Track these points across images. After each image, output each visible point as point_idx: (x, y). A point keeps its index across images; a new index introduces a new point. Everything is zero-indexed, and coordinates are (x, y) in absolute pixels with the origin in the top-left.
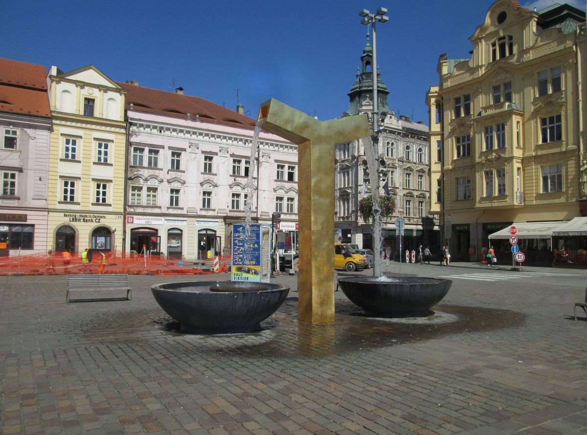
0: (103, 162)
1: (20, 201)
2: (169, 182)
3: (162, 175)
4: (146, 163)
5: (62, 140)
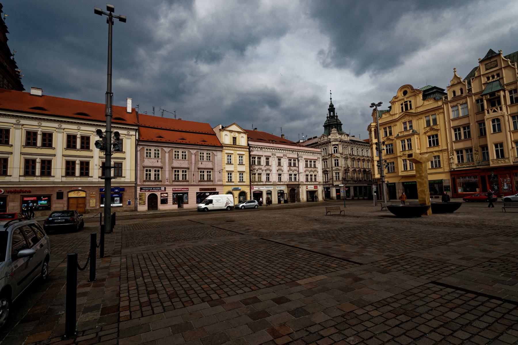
0: (241, 164)
1: (213, 182)
2: (266, 170)
3: (263, 168)
4: (256, 163)
5: (226, 156)
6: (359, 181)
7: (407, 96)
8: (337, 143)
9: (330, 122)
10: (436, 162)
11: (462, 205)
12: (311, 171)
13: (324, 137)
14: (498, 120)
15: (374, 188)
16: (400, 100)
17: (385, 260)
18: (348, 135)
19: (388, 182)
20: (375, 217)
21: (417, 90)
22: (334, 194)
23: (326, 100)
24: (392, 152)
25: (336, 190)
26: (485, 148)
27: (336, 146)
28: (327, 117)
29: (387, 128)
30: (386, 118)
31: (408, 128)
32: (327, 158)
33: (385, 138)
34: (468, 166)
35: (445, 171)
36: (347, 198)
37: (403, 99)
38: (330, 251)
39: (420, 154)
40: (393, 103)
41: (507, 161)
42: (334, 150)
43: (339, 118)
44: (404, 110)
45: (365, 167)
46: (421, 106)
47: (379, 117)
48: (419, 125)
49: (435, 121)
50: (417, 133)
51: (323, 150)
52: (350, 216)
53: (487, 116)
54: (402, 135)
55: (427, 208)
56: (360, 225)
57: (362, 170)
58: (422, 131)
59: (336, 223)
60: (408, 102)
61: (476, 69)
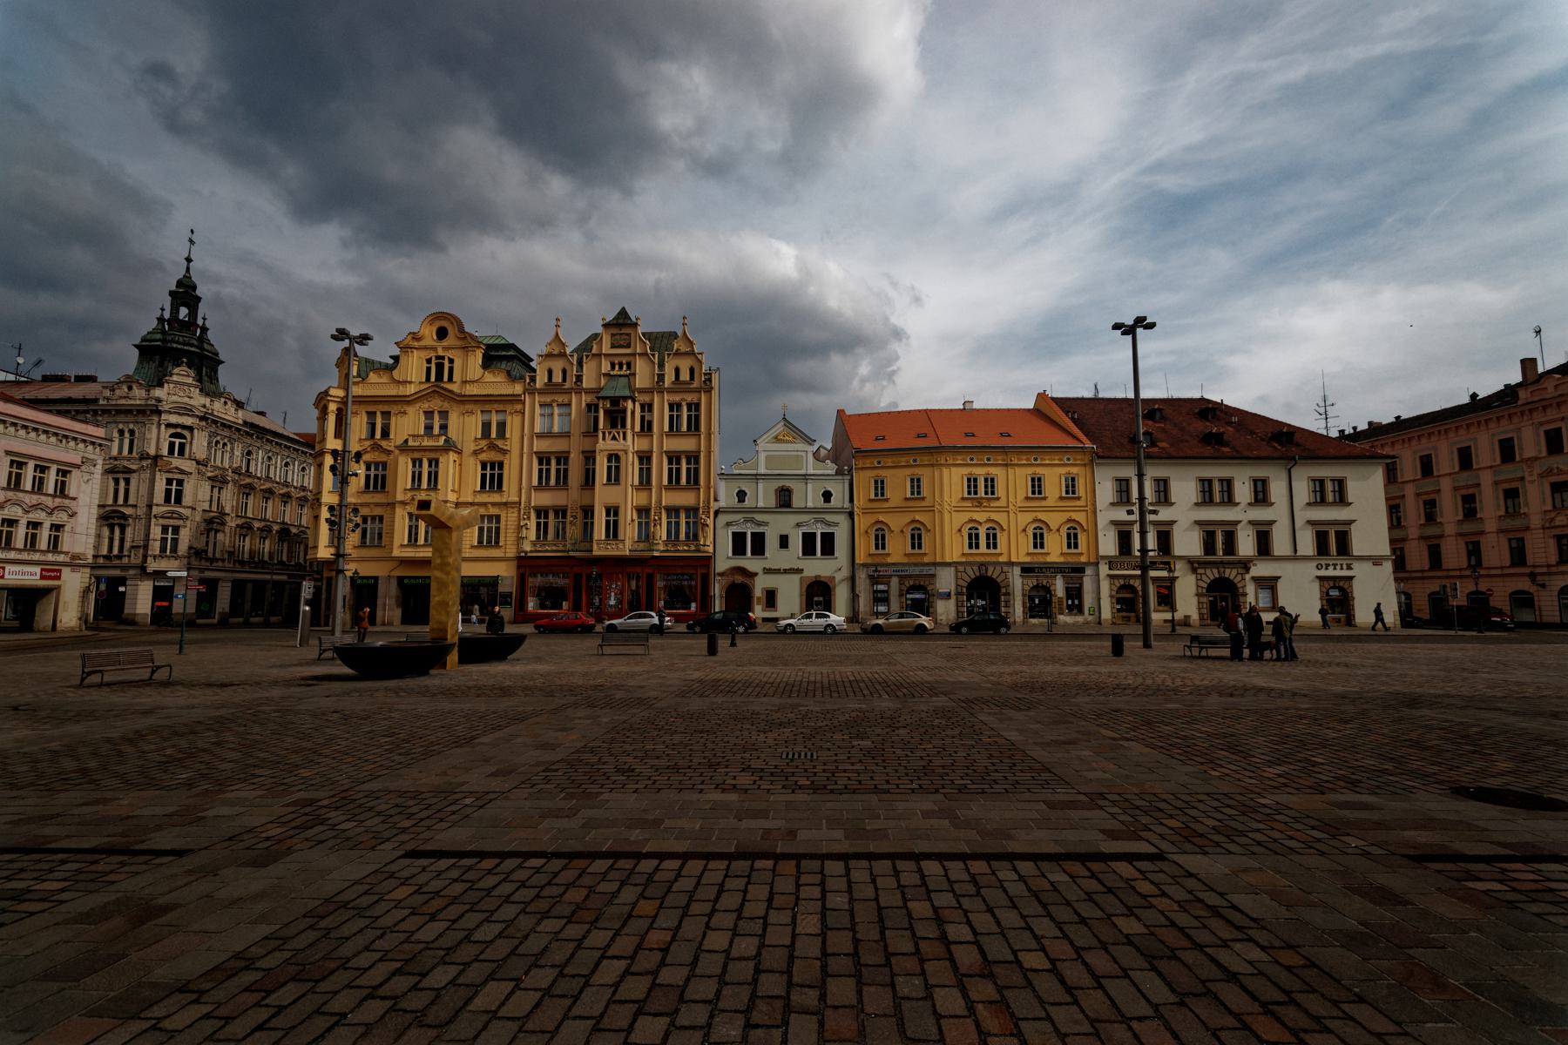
6: (256, 562)
7: (445, 343)
8: (188, 421)
9: (172, 341)
10: (490, 530)
11: (527, 642)
12: (36, 507)
13: (130, 388)
14: (618, 458)
15: (307, 589)
16: (425, 348)
17: (281, 820)
18: (239, 405)
19: (356, 572)
20: (288, 683)
21: (471, 336)
22: (142, 600)
23: (170, 252)
24: (383, 486)
25: (156, 589)
26: (588, 511)
27: (179, 431)
28: (161, 320)
29: (379, 414)
30: (377, 386)
31: (436, 430)
32: (134, 467)
33: (368, 443)
34: (554, 548)
35: (508, 555)
36: (199, 621)
37: (434, 349)
38: (49, 831)
39: (457, 505)
40: (405, 348)
41: (621, 546)
42: (172, 445)
43: (210, 335)
44: (433, 378)
45: (287, 520)
46: (477, 381)
47: (359, 375)
48: (466, 427)
49: (502, 426)
50: (456, 447)
51: (116, 434)
52: (192, 685)
53: (601, 445)
54: (417, 444)
55: (447, 649)
56: (223, 712)
57: (276, 528)
58: (469, 447)
59: (115, 716)
60: (446, 359)
61: (595, 336)
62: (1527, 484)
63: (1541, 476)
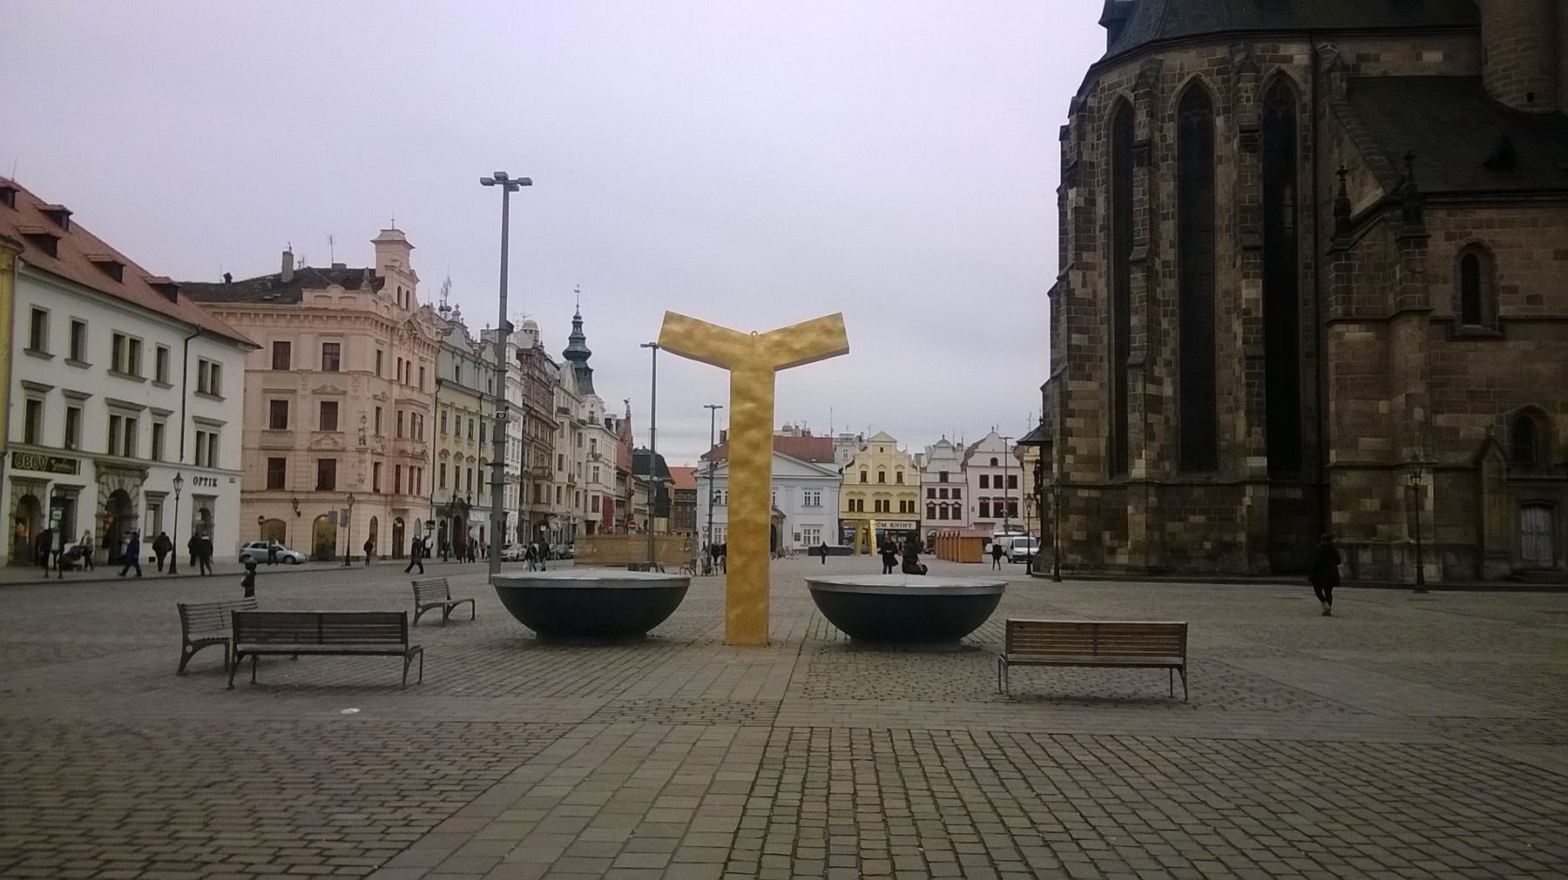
62: (298, 397)
63: (314, 392)
